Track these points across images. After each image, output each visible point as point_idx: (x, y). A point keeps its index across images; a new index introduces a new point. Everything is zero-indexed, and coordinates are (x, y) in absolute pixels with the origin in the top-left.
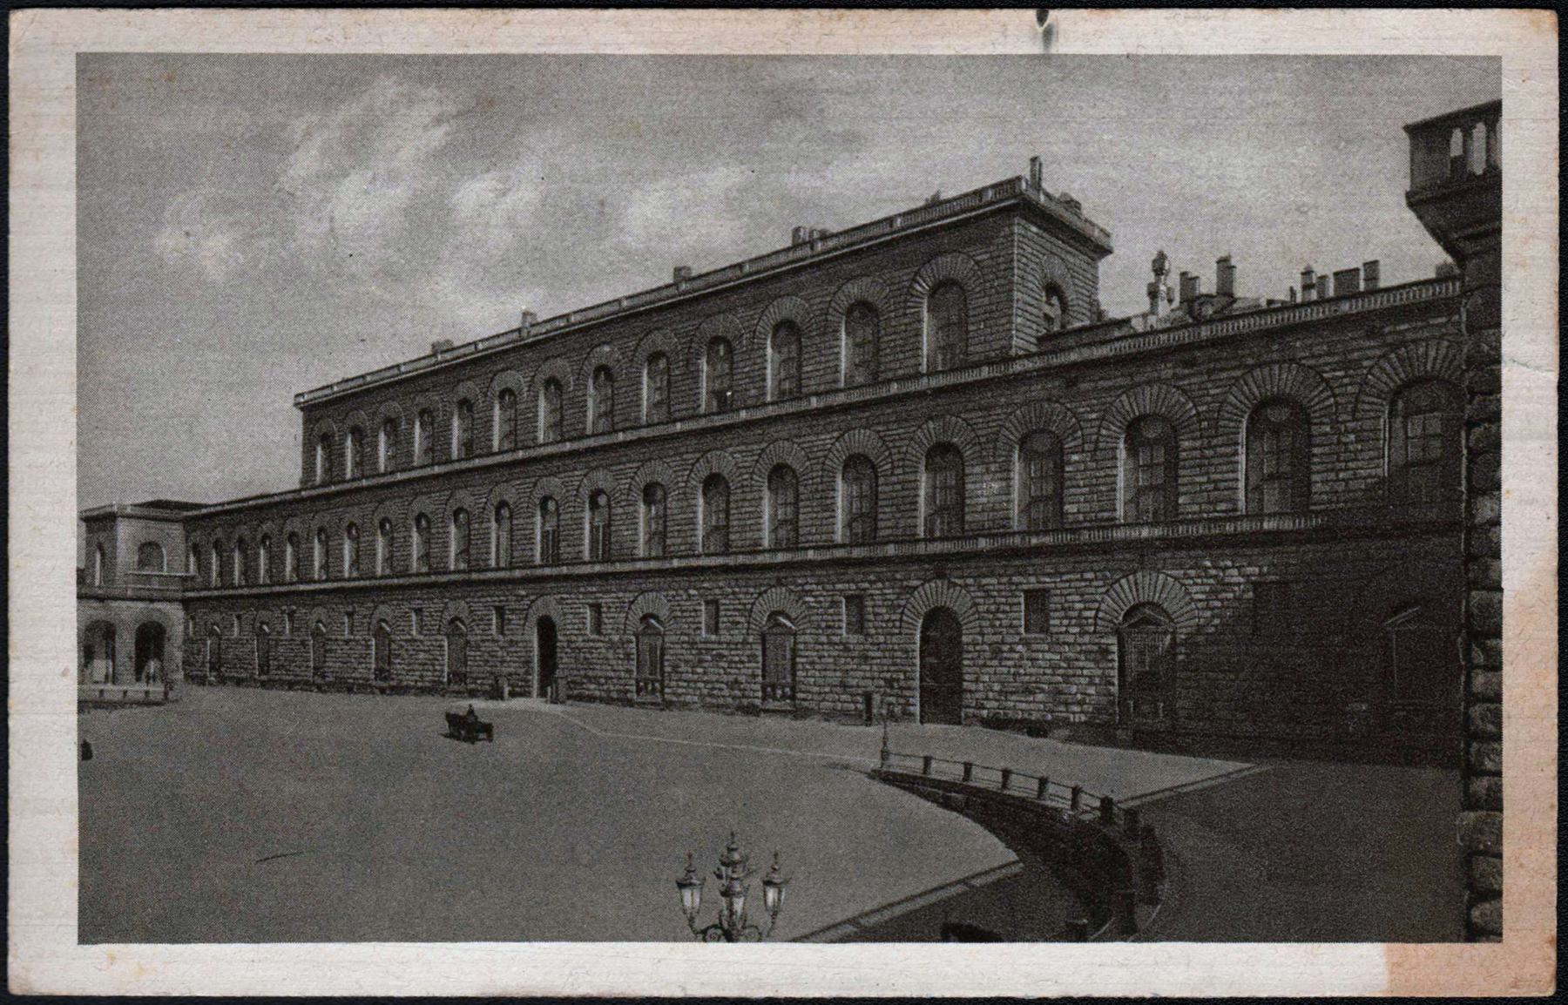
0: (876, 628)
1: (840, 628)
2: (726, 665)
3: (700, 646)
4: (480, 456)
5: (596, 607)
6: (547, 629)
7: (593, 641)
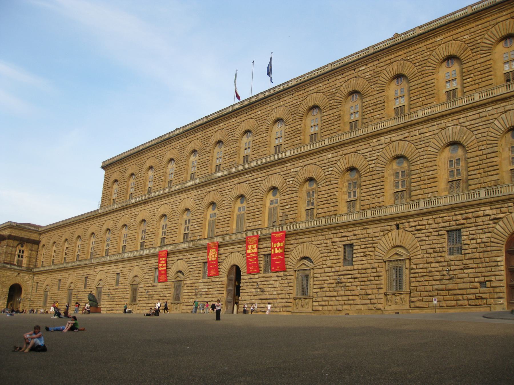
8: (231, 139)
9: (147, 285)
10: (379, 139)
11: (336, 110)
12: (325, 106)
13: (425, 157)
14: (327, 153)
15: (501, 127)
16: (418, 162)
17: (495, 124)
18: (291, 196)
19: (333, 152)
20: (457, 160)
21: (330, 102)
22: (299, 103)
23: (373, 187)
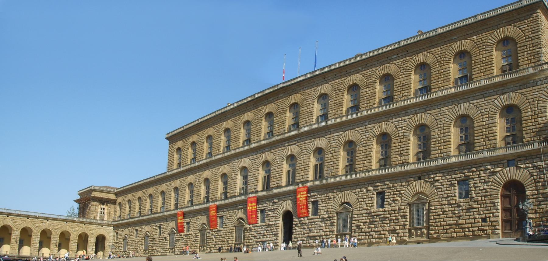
0: (476, 194)
1: (455, 196)
3: (373, 214)
7: (313, 219)
8: (280, 110)
10: (406, 111)
11: (371, 88)
12: (364, 84)
13: (442, 125)
14: (365, 122)
15: (499, 105)
16: (437, 130)
17: (495, 102)
18: (334, 154)
19: (370, 120)
20: (465, 128)
21: (367, 82)
22: (341, 82)
23: (401, 148)
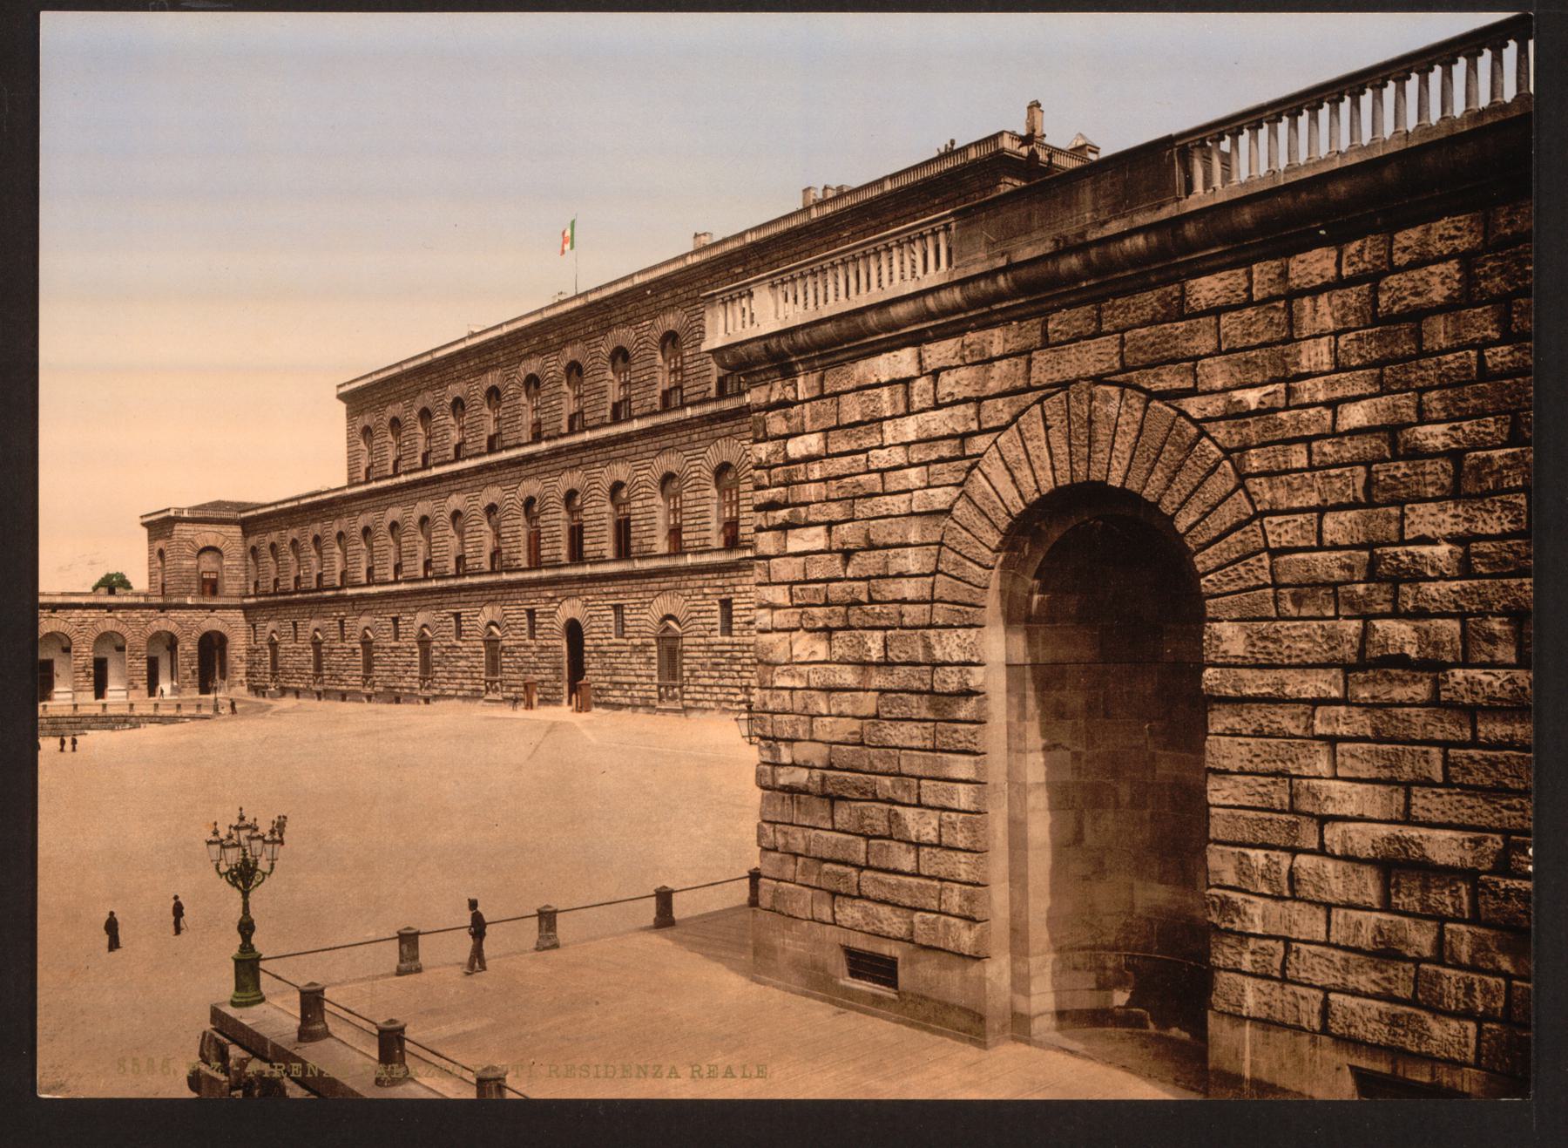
2: (739, 668)
4: (437, 465)
5: (618, 609)
6: (574, 631)
9: (445, 644)
